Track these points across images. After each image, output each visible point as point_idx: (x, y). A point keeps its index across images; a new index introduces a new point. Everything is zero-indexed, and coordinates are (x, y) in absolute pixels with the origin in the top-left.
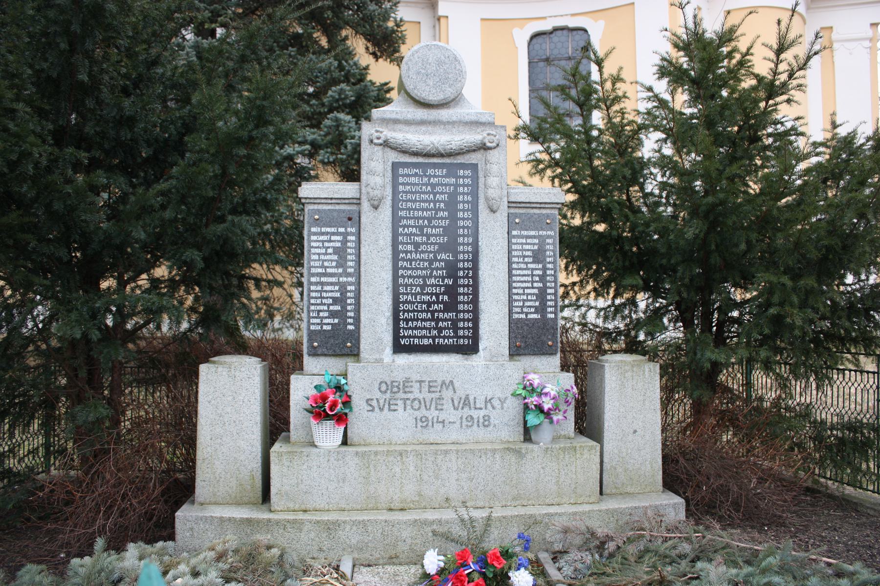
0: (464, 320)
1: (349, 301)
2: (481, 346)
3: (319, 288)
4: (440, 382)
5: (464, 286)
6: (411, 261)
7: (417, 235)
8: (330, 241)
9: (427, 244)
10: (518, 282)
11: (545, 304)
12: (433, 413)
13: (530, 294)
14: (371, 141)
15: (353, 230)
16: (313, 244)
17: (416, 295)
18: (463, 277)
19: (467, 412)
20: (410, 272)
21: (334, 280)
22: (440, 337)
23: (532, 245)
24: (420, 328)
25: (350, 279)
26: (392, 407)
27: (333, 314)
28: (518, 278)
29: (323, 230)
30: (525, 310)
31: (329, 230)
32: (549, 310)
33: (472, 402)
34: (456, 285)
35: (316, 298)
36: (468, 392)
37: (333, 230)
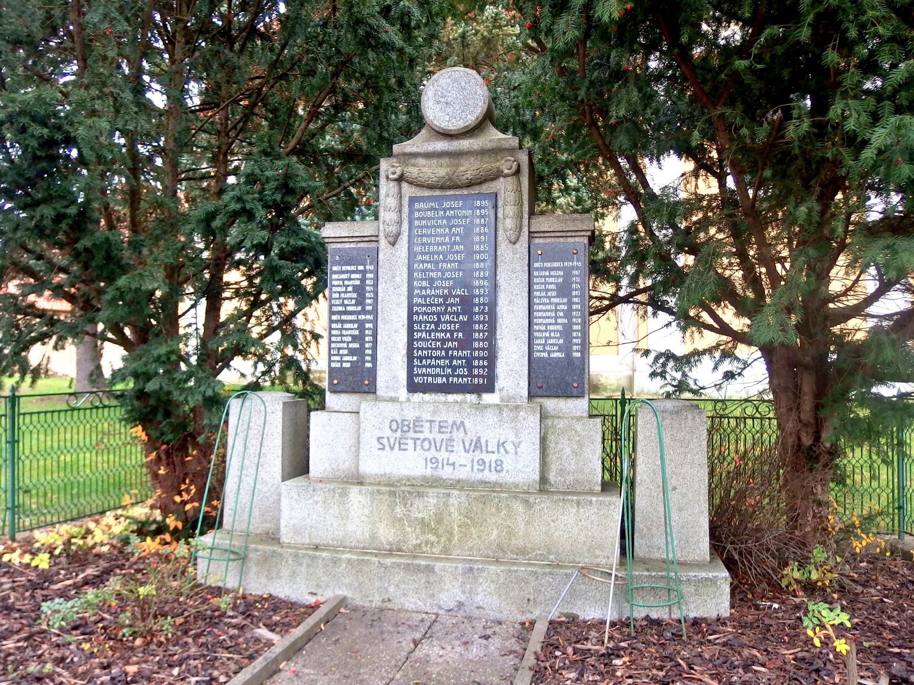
0: (479, 358)
1: (367, 339)
2: (498, 385)
3: (339, 326)
4: (450, 423)
5: (479, 322)
6: (425, 297)
7: (432, 271)
8: (350, 279)
9: (442, 279)
10: (540, 318)
11: (571, 342)
12: (443, 455)
13: (554, 331)
14: (387, 178)
15: (372, 268)
16: (334, 283)
17: (430, 332)
18: (479, 314)
19: (478, 456)
20: (424, 309)
21: (353, 317)
22: (453, 376)
23: (557, 278)
24: (433, 366)
25: (368, 317)
26: (403, 447)
27: (352, 352)
28: (540, 314)
29: (344, 268)
30: (548, 348)
31: (349, 268)
32: (575, 348)
33: (483, 444)
34: (471, 322)
35: (336, 336)
36: (480, 434)
37: (353, 268)
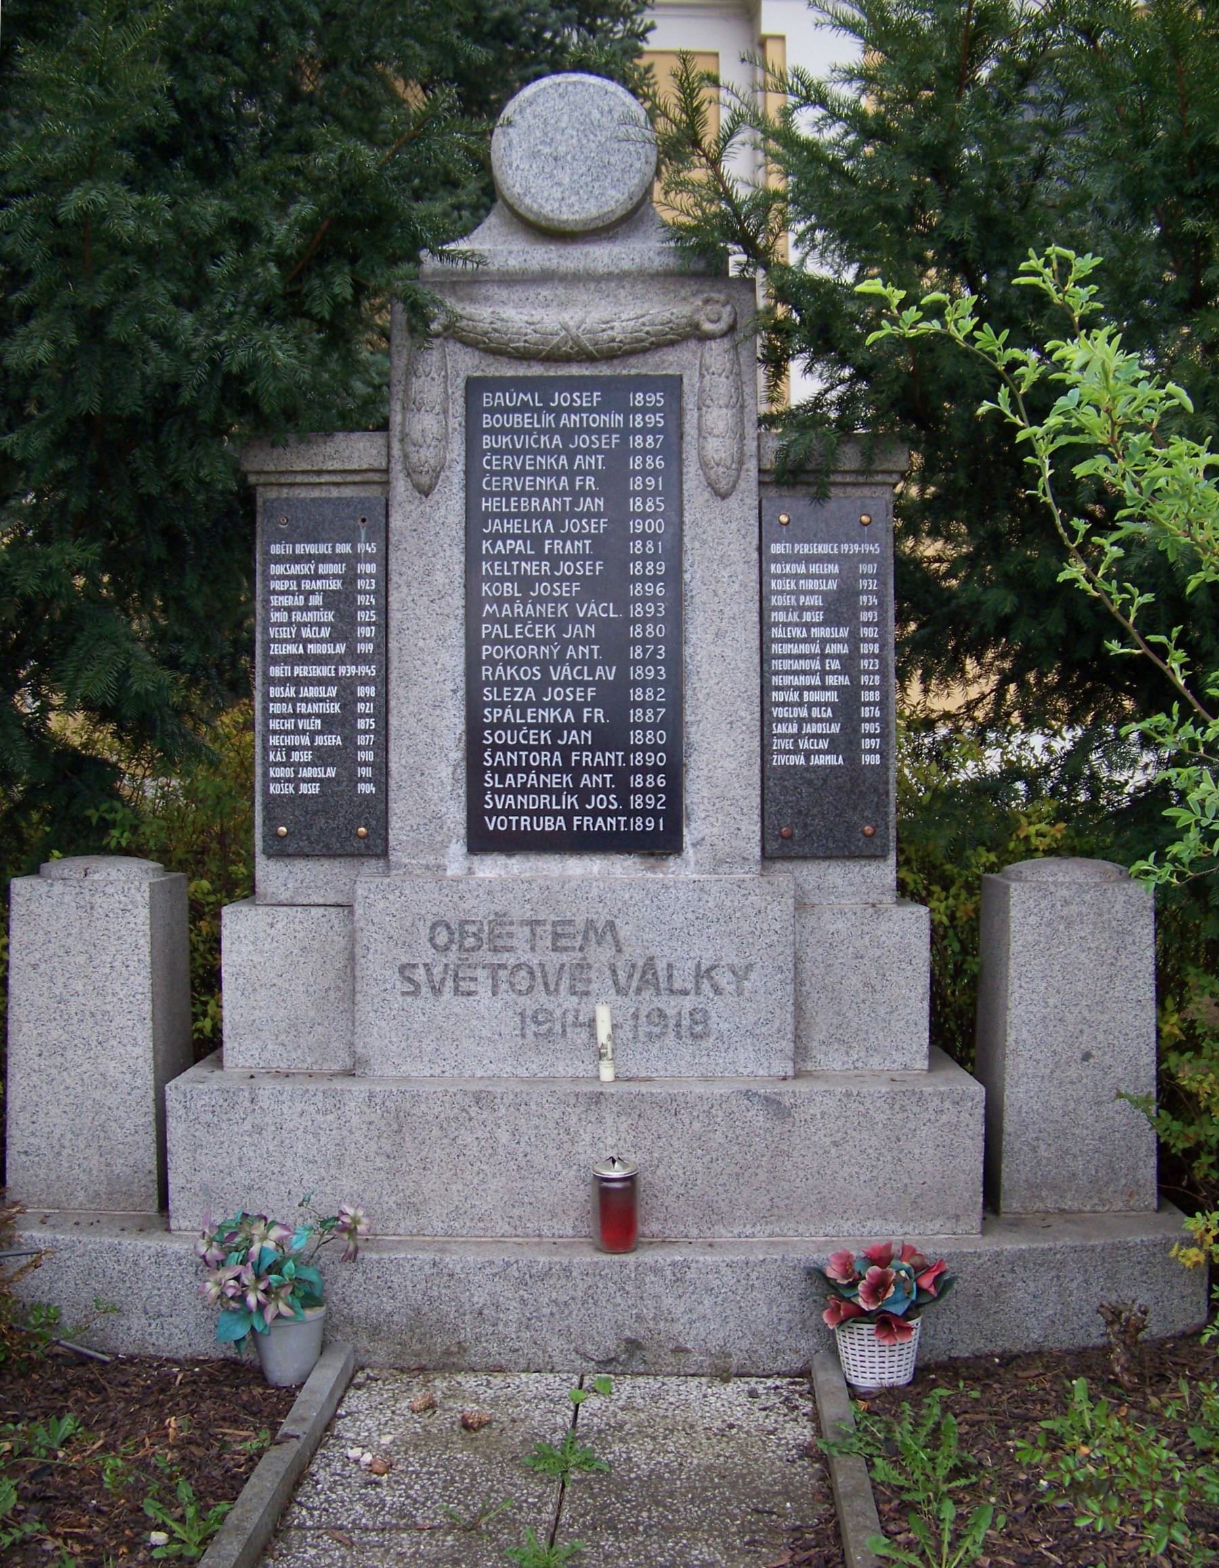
0: (644, 770)
1: (361, 724)
3: (290, 692)
5: (644, 684)
6: (511, 622)
7: (527, 558)
8: (316, 576)
9: (551, 579)
11: (856, 730)
15: (371, 548)
17: (524, 706)
18: (643, 662)
22: (583, 812)
23: (822, 581)
25: (364, 670)
26: (464, 986)
27: (322, 757)
28: (787, 664)
29: (300, 549)
30: (804, 744)
31: (312, 549)
32: (866, 744)
33: (662, 975)
34: (624, 683)
35: (282, 716)
36: (654, 951)
37: (323, 549)
